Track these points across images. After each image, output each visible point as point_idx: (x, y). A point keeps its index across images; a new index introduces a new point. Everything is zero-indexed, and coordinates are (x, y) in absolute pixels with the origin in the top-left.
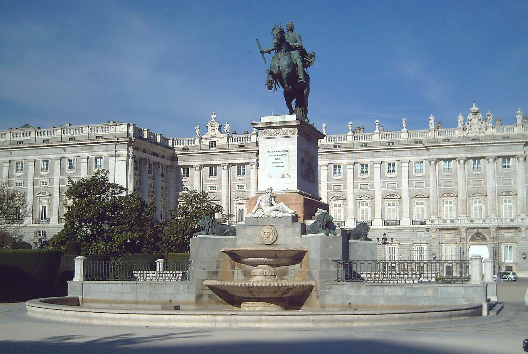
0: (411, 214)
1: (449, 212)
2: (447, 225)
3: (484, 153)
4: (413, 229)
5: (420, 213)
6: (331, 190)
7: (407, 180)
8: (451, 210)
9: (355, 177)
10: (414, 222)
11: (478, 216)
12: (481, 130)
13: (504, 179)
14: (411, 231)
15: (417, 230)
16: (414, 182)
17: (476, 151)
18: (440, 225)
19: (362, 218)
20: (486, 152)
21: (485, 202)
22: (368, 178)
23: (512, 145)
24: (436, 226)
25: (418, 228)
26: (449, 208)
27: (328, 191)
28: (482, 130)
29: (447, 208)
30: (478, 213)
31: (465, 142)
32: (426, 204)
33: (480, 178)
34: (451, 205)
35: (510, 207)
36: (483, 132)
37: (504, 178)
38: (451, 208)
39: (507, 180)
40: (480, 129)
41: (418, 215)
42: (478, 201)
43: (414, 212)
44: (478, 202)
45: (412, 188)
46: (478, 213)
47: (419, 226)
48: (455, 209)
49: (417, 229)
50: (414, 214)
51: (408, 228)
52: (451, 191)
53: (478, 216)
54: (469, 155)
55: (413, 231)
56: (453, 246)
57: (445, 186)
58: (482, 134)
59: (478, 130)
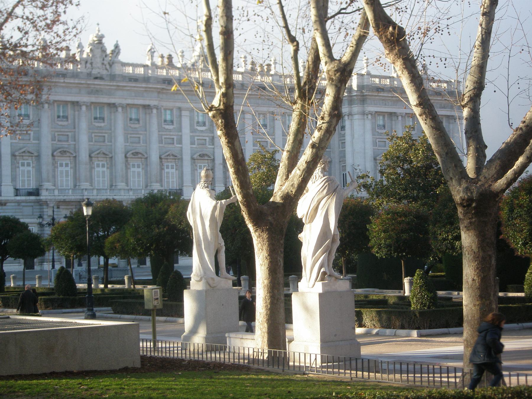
0: (14, 179)
1: (64, 179)
2: (71, 197)
3: (112, 98)
4: (19, 203)
5: (26, 179)
8: (67, 176)
9: (160, 129)
10: (17, 192)
11: (101, 185)
12: (104, 66)
13: (133, 136)
14: (15, 206)
17: (102, 95)
18: (60, 198)
19: (23, 185)
20: (115, 98)
21: (108, 166)
23: (146, 91)
24: (57, 198)
25: (23, 201)
26: (64, 172)
27: (212, 147)
28: (105, 65)
29: (62, 172)
30: (64, 180)
31: (116, 83)
32: (34, 165)
33: (102, 133)
34: (67, 169)
35: (139, 174)
36: (107, 69)
37: (131, 134)
38: (67, 172)
39: (201, 139)
40: (103, 64)
41: (23, 181)
42: (136, 164)
43: (18, 177)
44: (26, 164)
45: (14, 141)
46: (64, 180)
47: (23, 198)
48: (108, 174)
49: (24, 202)
50: (18, 179)
51: (12, 201)
52: (67, 148)
53: (101, 185)
55: (19, 205)
56: (33, 228)
57: (59, 141)
59: (99, 65)
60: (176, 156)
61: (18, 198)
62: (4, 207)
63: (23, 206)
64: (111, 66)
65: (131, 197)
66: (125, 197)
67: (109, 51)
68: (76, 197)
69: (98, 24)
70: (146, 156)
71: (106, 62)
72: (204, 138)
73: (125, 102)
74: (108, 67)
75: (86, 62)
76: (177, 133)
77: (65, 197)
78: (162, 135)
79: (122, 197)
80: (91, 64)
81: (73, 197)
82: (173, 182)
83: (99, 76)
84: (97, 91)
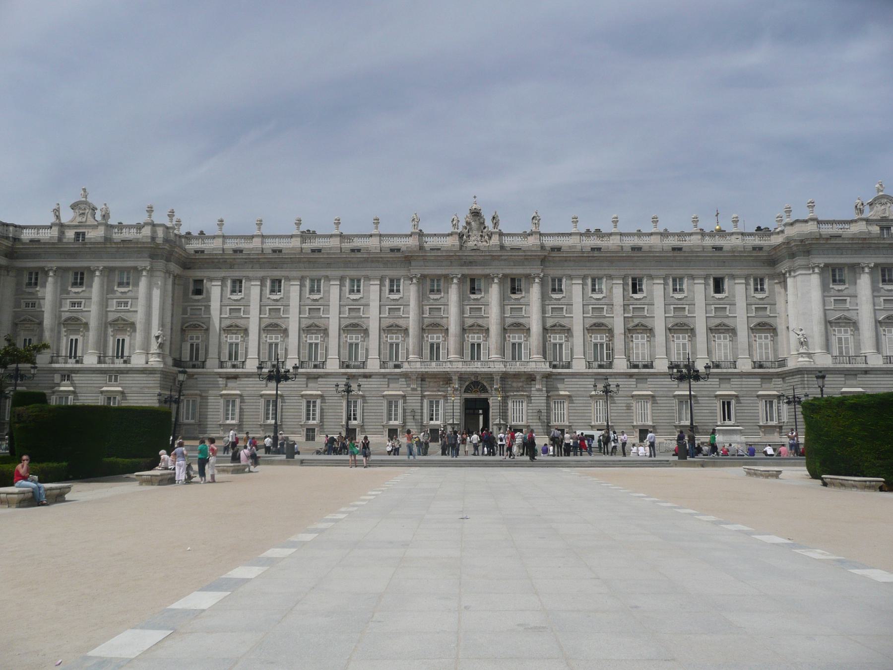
2: (433, 370)
4: (384, 375)
6: (265, 314)
7: (378, 303)
15: (389, 377)
16: (387, 307)
18: (421, 370)
20: (490, 269)
22: (321, 298)
40: (481, 236)
45: (384, 316)
54: (426, 272)
58: (485, 243)
59: (479, 238)
60: (564, 327)
61: (383, 371)
62: (368, 380)
63: (389, 379)
64: (490, 238)
65: (501, 370)
66: (494, 370)
67: (489, 223)
68: (439, 370)
69: (475, 197)
70: (528, 327)
71: (483, 234)
72: (601, 306)
73: (501, 273)
74: (486, 237)
75: (463, 235)
76: (566, 302)
77: (427, 370)
78: (628, 305)
79: (490, 370)
80: (469, 236)
81: (436, 370)
82: (643, 354)
83: (475, 248)
84: (470, 262)
